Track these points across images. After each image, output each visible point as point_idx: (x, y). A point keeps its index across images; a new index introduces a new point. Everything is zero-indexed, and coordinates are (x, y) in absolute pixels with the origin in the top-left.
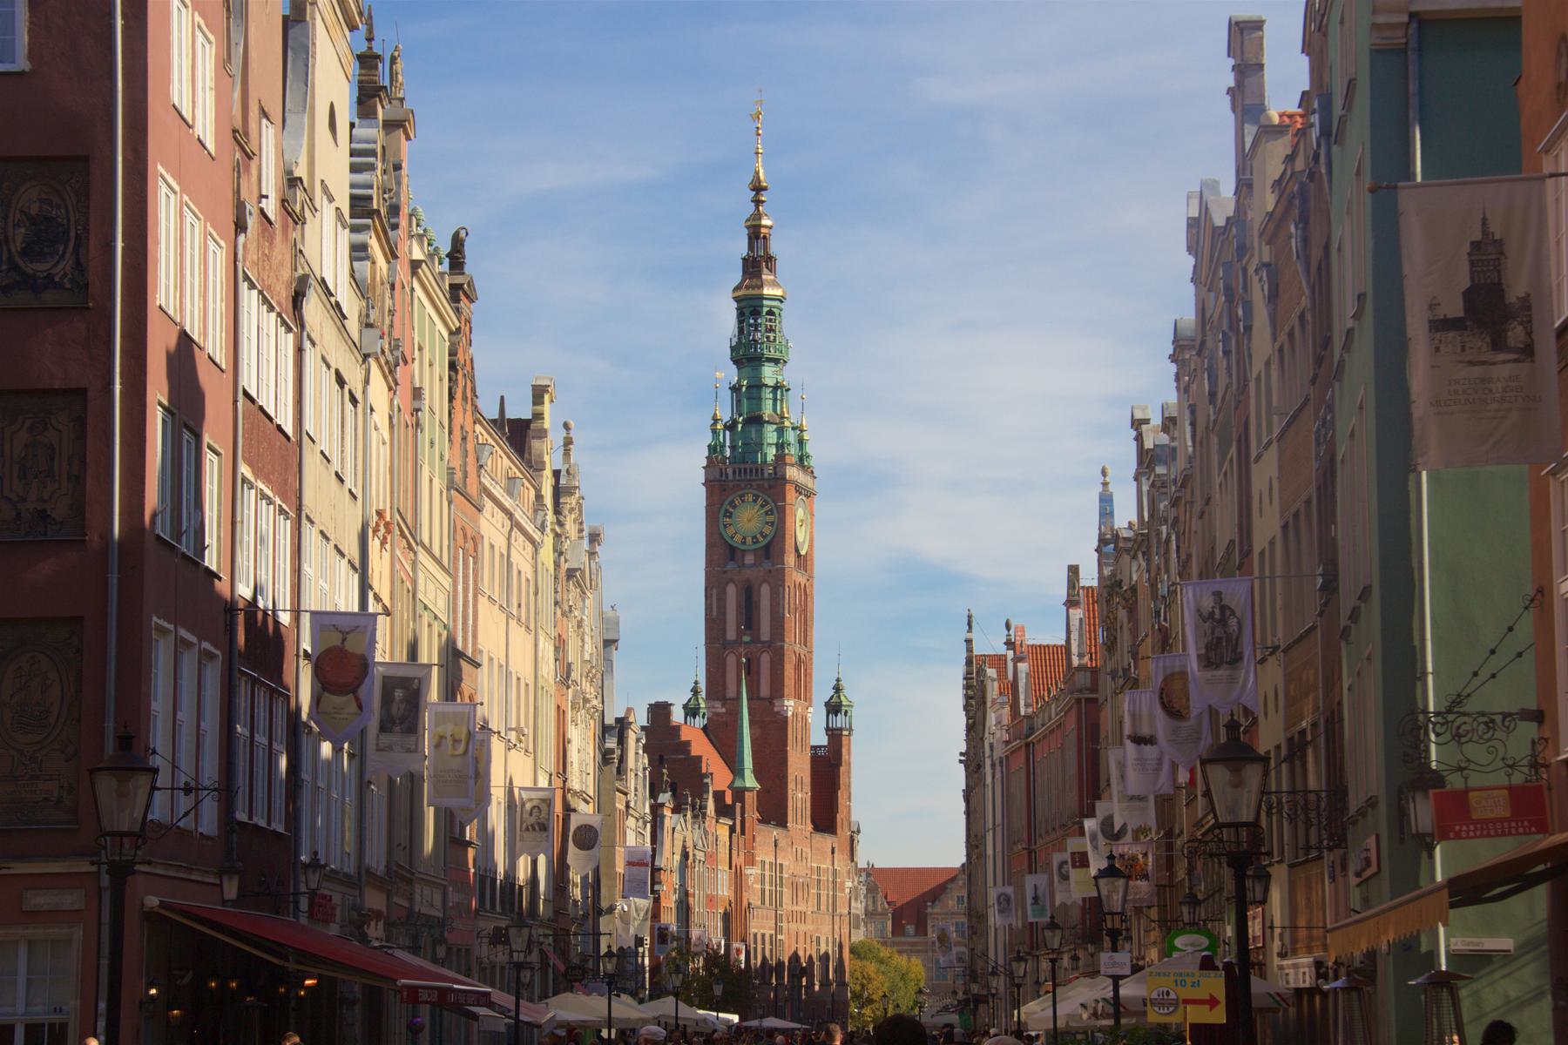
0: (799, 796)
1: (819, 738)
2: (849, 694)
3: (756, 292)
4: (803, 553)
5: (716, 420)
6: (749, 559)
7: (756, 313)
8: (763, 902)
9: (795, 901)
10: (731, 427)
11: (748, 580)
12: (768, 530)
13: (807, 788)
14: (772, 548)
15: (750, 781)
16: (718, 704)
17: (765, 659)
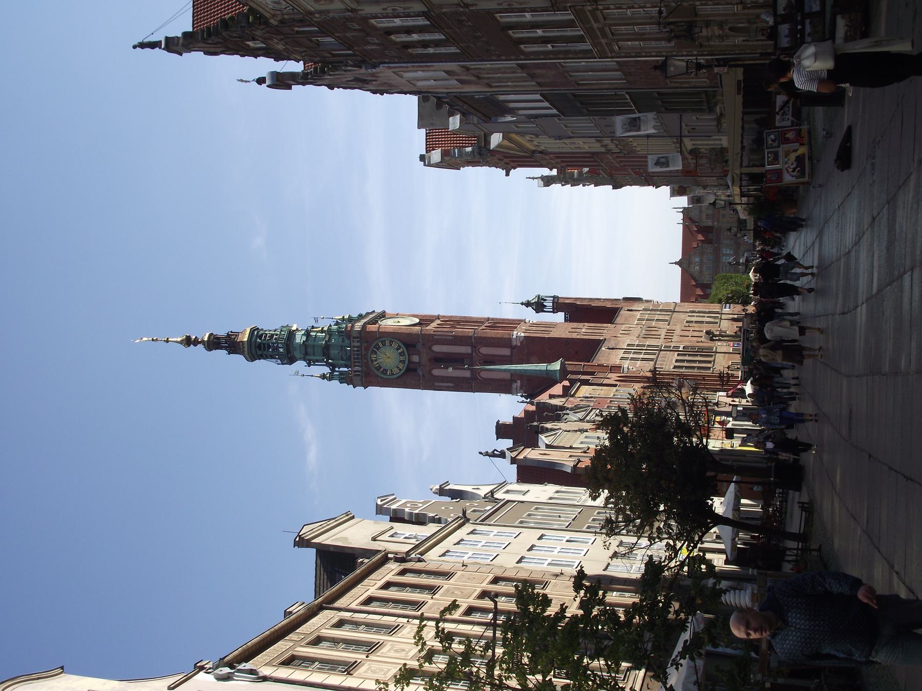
0: (584, 331)
1: (560, 317)
2: (531, 297)
3: (246, 346)
4: (417, 321)
5: (323, 377)
6: (416, 358)
7: (259, 346)
8: (652, 360)
10: (333, 367)
11: (430, 360)
12: (395, 345)
13: (581, 325)
14: (408, 341)
15: (556, 366)
16: (514, 386)
17: (484, 350)
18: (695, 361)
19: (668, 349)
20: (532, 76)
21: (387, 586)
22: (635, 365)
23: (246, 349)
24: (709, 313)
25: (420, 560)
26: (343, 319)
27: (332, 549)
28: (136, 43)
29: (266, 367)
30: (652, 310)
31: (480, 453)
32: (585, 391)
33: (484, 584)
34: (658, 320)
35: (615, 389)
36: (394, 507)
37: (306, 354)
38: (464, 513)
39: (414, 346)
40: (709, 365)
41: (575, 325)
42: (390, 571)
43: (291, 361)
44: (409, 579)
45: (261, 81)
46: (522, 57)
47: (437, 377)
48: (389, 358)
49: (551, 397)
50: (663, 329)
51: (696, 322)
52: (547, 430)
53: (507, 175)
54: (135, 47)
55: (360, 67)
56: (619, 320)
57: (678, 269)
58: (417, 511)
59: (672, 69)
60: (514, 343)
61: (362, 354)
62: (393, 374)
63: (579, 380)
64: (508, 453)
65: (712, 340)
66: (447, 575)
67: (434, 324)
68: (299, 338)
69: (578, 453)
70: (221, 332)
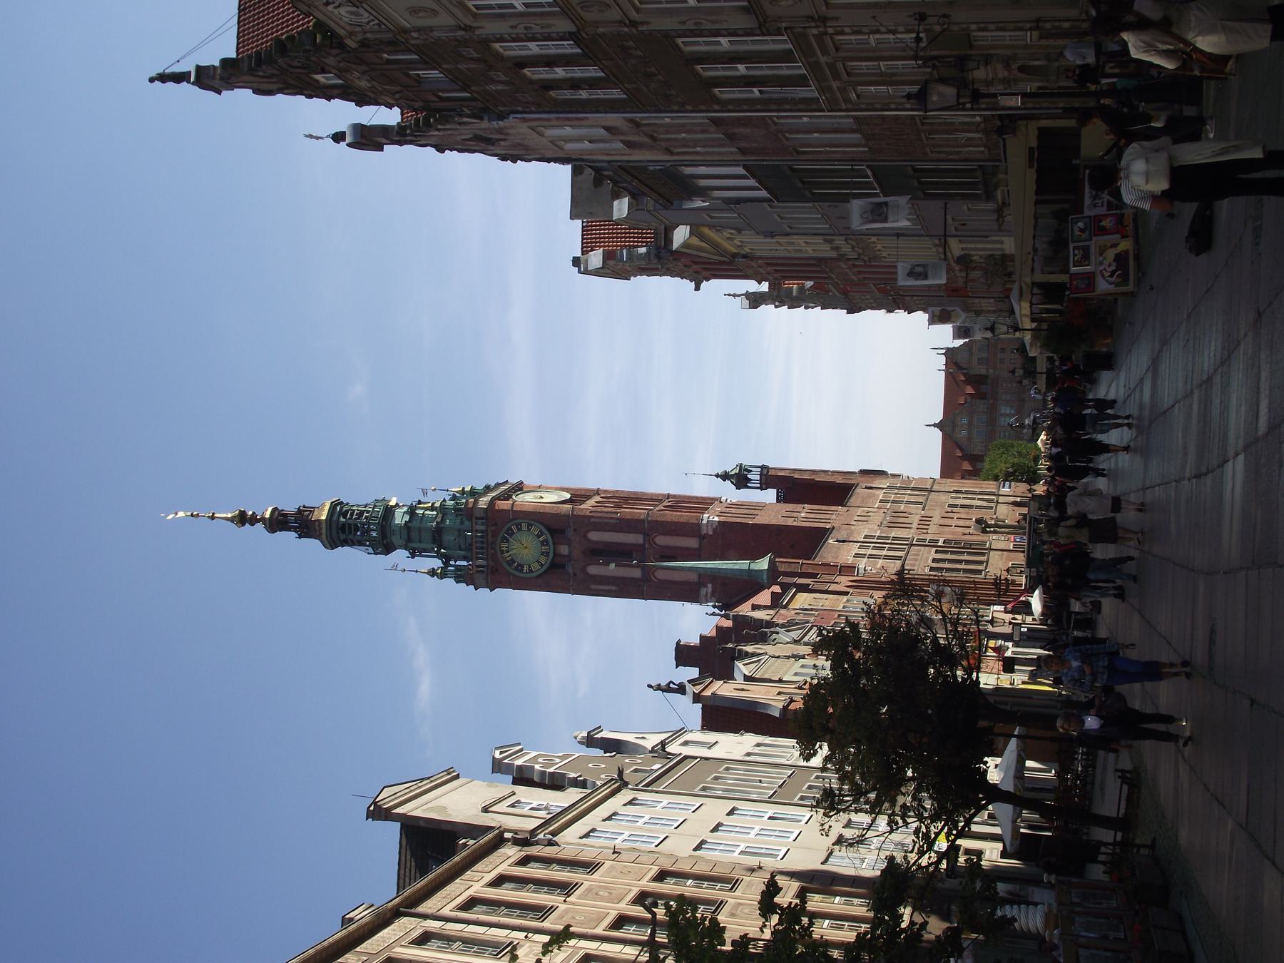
0: (803, 515)
1: (770, 495)
2: (731, 467)
3: (324, 526)
4: (568, 496)
5: (432, 573)
6: (564, 550)
7: (343, 528)
8: (899, 558)
9: (907, 526)
10: (446, 559)
13: (799, 507)
14: (553, 525)
15: (763, 564)
16: (703, 591)
17: (661, 540)
18: (960, 561)
19: (921, 543)
20: (731, 138)
21: (499, 881)
22: (874, 565)
23: (324, 531)
24: (981, 493)
25: (551, 843)
26: (463, 492)
27: (422, 824)
28: (153, 74)
29: (352, 557)
30: (900, 488)
31: (650, 686)
32: (803, 600)
33: (644, 882)
34: (908, 502)
35: (845, 598)
36: (519, 762)
37: (409, 540)
38: (621, 773)
39: (562, 532)
40: (980, 567)
41: (791, 507)
42: (505, 860)
43: (388, 549)
44: (533, 871)
45: (338, 137)
46: (716, 107)
47: (593, 577)
48: (526, 548)
49: (755, 607)
50: (916, 514)
51: (962, 506)
52: (747, 655)
53: (697, 288)
54: (152, 80)
55: (481, 118)
56: (852, 501)
57: (938, 435)
58: (552, 770)
59: (935, 98)
60: (704, 531)
61: (487, 541)
62: (531, 571)
63: (795, 585)
64: (689, 688)
65: (984, 531)
66: (590, 866)
67: (591, 502)
68: (400, 518)
69: (790, 689)
70: (290, 506)
